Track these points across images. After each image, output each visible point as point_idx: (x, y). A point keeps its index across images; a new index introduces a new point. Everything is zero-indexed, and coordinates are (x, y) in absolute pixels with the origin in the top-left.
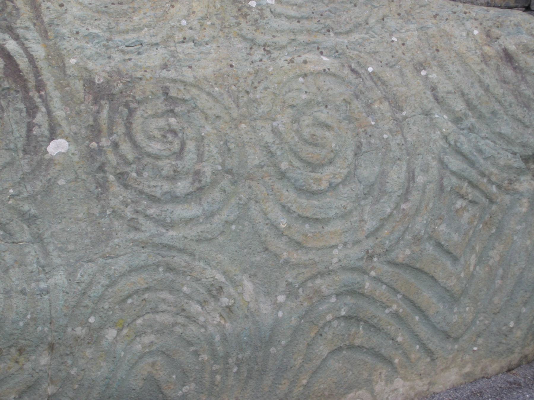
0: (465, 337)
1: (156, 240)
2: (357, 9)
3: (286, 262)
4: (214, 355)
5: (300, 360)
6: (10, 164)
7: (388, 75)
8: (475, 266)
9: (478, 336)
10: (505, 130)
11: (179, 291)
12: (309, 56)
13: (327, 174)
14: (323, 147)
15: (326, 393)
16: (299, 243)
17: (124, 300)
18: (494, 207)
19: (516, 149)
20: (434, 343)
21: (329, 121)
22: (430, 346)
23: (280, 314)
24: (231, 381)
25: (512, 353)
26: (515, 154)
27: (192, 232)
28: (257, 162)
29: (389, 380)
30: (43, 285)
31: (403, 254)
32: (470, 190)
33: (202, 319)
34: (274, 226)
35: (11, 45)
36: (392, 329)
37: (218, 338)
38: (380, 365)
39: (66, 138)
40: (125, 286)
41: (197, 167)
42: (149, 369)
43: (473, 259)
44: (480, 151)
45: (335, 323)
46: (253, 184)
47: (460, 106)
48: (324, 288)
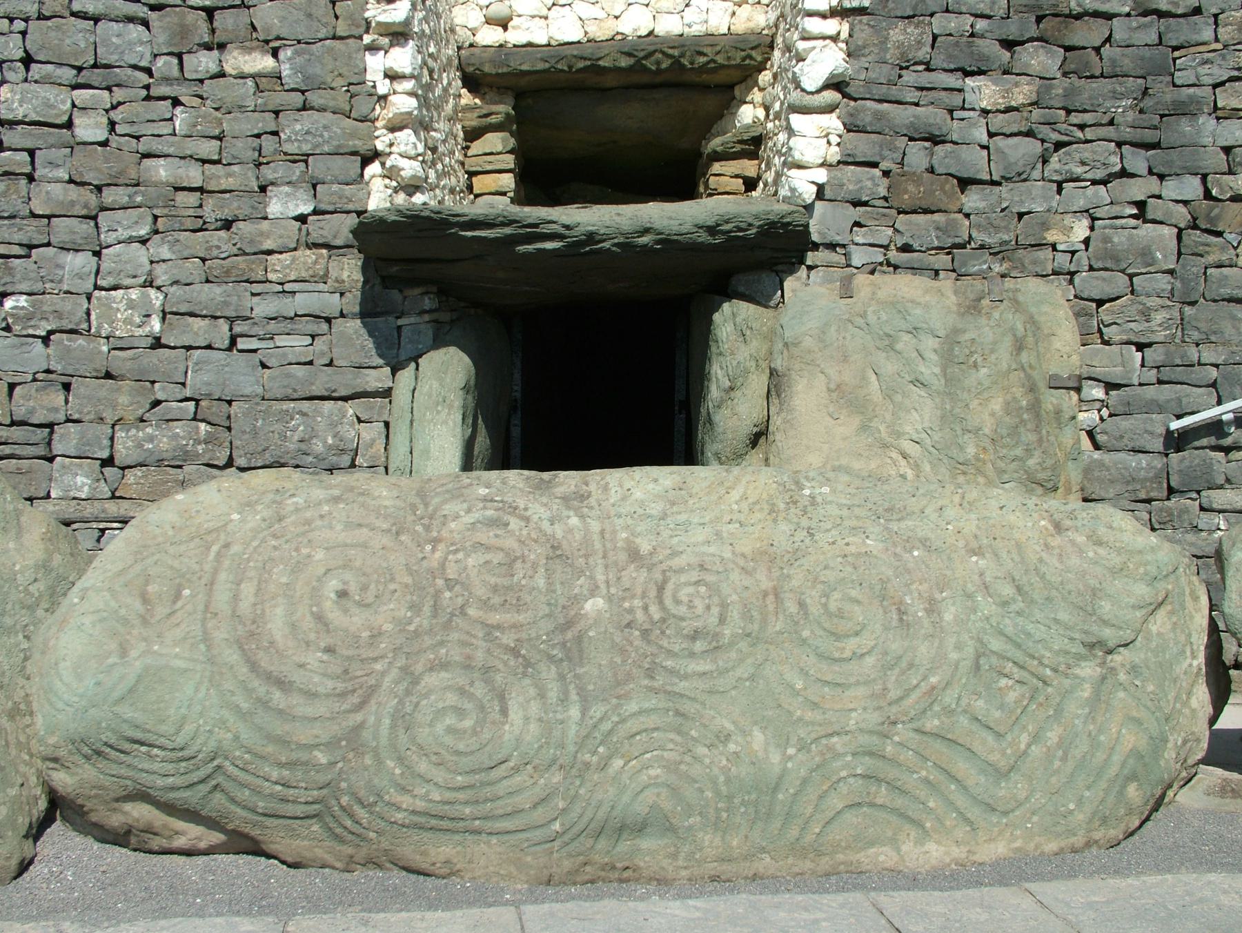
0: (1017, 813)
1: (669, 688)
2: (914, 499)
3: (800, 719)
4: (717, 793)
5: (810, 810)
6: (549, 616)
8: (1029, 746)
9: (1033, 814)
10: (1063, 616)
11: (687, 734)
12: (850, 539)
13: (851, 644)
14: (850, 619)
15: (843, 844)
16: (815, 704)
17: (633, 736)
18: (1050, 690)
19: (1077, 636)
20: (974, 813)
21: (860, 597)
22: (969, 815)
23: (790, 765)
24: (738, 819)
25: (1075, 835)
26: (1072, 639)
28: (778, 628)
29: (919, 842)
30: (559, 716)
31: (932, 724)
32: (1015, 670)
33: (707, 761)
34: (791, 687)
36: (922, 793)
37: (722, 779)
38: (907, 827)
39: (603, 597)
40: (632, 725)
41: (718, 630)
42: (655, 798)
43: (1024, 739)
44: (1028, 635)
45: (851, 780)
46: (772, 648)
47: (1008, 590)
48: (838, 747)
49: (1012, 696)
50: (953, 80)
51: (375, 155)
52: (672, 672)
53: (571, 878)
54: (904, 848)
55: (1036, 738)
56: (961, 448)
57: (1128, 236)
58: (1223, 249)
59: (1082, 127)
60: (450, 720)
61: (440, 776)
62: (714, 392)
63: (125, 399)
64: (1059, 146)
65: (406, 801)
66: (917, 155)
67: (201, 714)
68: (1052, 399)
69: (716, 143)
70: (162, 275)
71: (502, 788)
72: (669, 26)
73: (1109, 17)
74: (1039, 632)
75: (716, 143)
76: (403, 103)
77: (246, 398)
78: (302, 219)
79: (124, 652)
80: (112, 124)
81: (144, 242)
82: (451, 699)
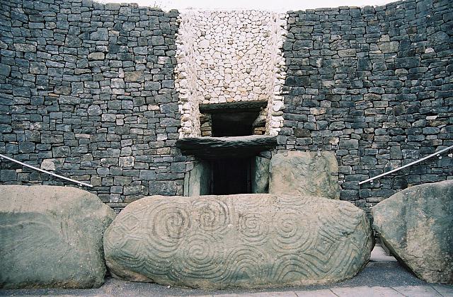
7: (308, 214)
20: (319, 273)
27: (256, 243)
31: (308, 252)
35: (225, 206)
40: (239, 253)
43: (330, 255)
49: (327, 245)
50: (307, 109)
51: (181, 127)
52: (249, 241)
53: (225, 288)
54: (303, 281)
55: (332, 255)
56: (312, 189)
57: (348, 141)
58: (368, 144)
59: (336, 118)
60: (197, 252)
61: (195, 265)
62: (257, 178)
63: (126, 180)
64: (332, 122)
65: (187, 271)
66: (300, 125)
67: (141, 251)
68: (333, 178)
69: (256, 123)
70: (134, 154)
71: (208, 268)
72: (245, 99)
73: (340, 95)
74: (332, 230)
75: (256, 123)
76: (186, 116)
77: (152, 180)
78: (165, 141)
79: (123, 236)
80: (124, 121)
81: (130, 146)
82: (198, 247)
